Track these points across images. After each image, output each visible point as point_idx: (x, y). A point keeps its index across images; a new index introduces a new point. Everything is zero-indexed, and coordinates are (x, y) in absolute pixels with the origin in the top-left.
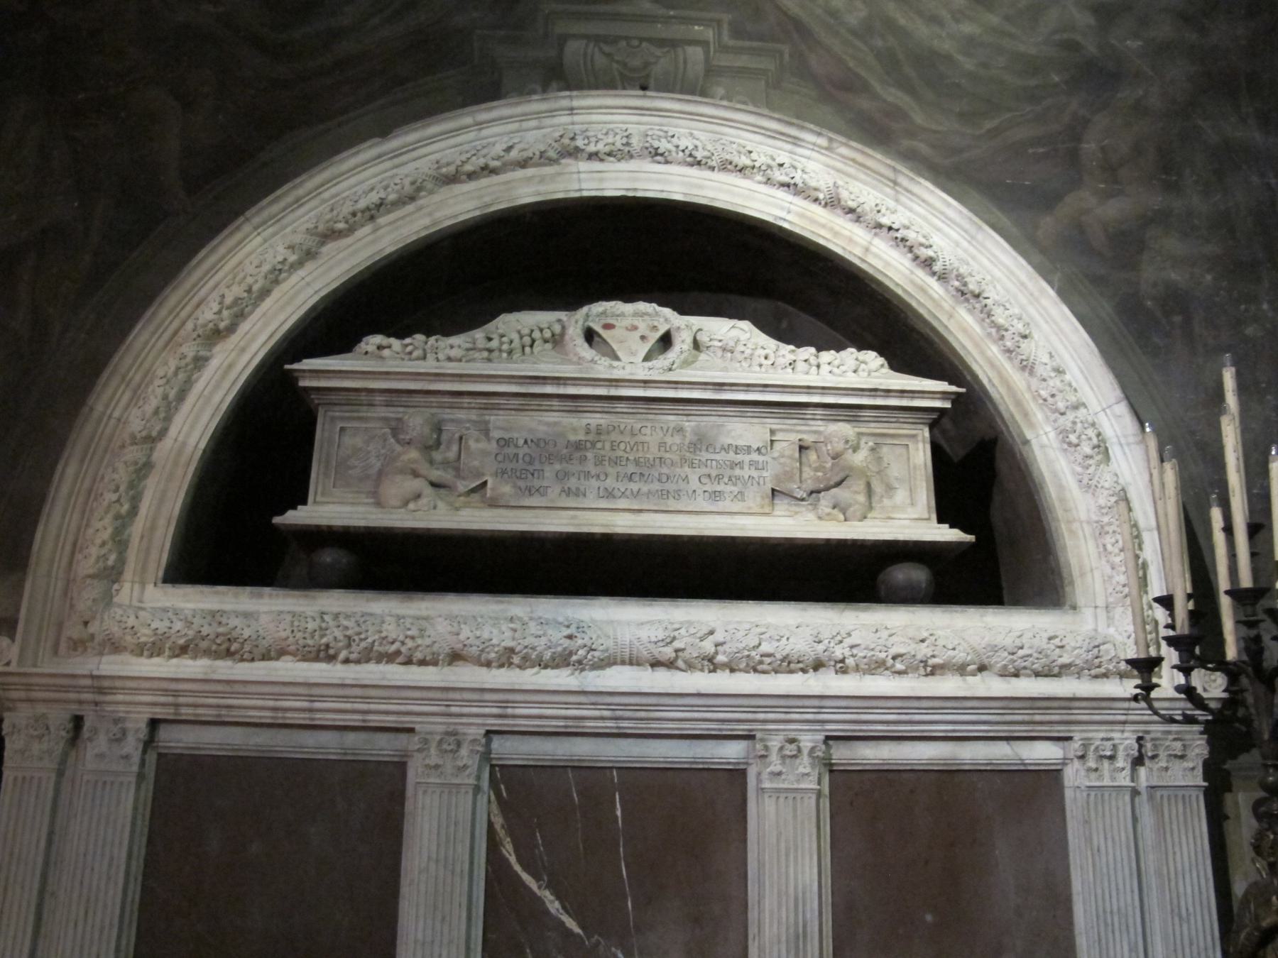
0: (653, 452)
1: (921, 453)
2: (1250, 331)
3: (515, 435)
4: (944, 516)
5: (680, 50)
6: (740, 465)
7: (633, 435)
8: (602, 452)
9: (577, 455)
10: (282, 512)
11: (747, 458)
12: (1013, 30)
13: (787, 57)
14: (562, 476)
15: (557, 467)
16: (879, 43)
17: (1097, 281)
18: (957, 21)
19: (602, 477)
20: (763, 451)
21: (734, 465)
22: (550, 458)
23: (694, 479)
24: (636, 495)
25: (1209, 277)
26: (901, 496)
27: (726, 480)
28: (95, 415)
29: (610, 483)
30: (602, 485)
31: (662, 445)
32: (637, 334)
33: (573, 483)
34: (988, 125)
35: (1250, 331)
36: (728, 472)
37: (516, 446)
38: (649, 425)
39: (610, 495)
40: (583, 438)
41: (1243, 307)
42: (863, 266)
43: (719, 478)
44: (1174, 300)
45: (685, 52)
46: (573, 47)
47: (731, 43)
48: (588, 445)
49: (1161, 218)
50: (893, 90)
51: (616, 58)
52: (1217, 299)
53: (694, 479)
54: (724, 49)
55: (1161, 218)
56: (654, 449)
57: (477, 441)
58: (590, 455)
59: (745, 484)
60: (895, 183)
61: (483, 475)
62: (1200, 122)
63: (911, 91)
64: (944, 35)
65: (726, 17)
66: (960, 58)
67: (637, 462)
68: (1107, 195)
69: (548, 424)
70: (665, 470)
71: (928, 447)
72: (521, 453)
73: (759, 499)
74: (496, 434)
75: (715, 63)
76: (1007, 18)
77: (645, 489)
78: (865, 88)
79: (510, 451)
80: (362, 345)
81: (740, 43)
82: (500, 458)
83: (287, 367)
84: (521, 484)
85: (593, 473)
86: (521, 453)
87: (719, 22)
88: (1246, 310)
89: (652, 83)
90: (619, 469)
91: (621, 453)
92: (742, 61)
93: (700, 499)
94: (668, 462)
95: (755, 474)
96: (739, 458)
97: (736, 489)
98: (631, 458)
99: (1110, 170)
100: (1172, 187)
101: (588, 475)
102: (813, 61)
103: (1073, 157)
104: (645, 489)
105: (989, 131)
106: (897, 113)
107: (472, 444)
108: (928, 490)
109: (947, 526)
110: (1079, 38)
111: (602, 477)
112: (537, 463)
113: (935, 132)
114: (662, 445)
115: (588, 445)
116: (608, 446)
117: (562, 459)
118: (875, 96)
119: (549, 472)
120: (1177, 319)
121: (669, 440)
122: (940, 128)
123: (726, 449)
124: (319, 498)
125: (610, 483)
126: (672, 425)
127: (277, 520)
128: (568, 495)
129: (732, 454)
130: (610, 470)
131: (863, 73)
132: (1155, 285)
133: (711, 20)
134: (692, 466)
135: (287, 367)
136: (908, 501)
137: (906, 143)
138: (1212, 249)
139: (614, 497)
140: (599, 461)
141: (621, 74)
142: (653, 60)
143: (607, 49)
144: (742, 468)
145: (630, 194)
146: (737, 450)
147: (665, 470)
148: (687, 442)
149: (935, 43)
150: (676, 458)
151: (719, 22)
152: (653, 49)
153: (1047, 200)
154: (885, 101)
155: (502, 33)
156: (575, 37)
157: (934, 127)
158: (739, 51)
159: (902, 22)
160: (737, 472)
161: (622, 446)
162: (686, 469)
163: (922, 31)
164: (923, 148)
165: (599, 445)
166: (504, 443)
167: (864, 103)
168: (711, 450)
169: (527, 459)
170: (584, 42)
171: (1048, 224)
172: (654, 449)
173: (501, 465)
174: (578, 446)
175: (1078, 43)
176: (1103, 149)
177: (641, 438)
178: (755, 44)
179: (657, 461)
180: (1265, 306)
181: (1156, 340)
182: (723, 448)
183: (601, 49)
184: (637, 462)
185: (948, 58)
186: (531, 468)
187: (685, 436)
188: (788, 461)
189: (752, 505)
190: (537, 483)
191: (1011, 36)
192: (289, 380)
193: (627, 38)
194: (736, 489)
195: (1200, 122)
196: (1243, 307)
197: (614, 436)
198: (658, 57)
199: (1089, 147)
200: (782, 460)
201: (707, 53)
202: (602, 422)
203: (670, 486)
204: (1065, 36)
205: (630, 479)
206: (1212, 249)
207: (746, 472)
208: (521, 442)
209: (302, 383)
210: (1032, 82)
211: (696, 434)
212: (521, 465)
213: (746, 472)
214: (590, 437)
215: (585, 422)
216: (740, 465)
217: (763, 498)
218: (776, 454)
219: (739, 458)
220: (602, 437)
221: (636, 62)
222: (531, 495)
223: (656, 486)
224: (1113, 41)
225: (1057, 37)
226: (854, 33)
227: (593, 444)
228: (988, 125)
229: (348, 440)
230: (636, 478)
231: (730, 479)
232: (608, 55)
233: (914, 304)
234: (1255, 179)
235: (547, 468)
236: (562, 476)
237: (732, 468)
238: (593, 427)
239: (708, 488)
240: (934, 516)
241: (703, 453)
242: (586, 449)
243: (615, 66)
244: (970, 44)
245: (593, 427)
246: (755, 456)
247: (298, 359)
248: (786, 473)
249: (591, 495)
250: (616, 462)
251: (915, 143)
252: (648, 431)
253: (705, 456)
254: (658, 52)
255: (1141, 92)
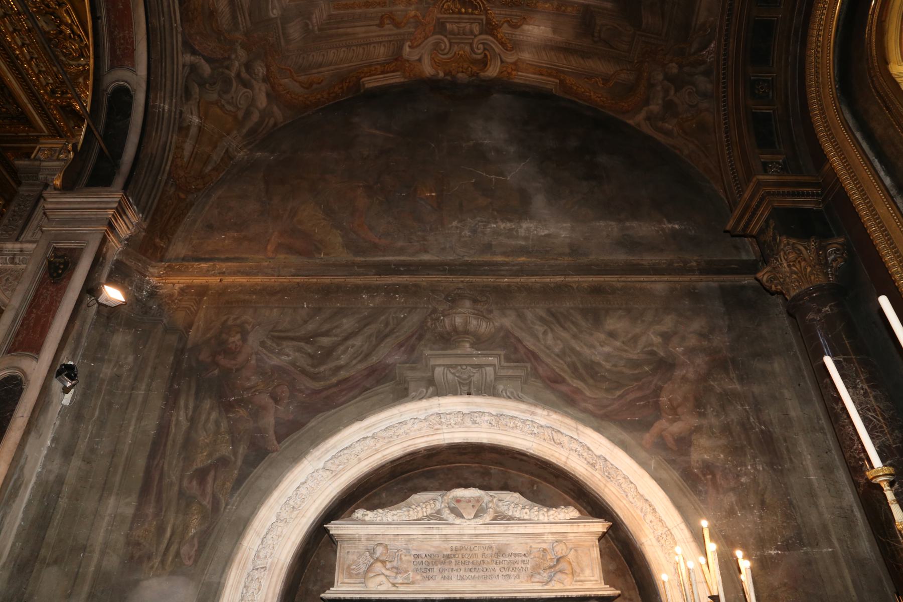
0: (480, 559)
1: (595, 552)
2: (743, 480)
3: (421, 553)
4: (608, 579)
5: (483, 369)
6: (517, 562)
7: (471, 551)
8: (458, 559)
9: (448, 561)
10: (324, 592)
11: (520, 559)
12: (626, 348)
13: (529, 369)
14: (441, 571)
15: (439, 566)
16: (569, 359)
17: (672, 462)
18: (602, 346)
19: (459, 570)
20: (527, 555)
21: (514, 562)
22: (436, 563)
23: (497, 569)
24: (473, 578)
25: (722, 456)
26: (588, 572)
27: (511, 569)
28: (244, 547)
29: (462, 573)
30: (458, 574)
31: (483, 554)
32: (471, 504)
33: (446, 574)
34: (618, 393)
35: (743, 480)
36: (512, 566)
37: (422, 558)
38: (478, 546)
39: (462, 578)
40: (449, 552)
41: (739, 469)
42: (565, 468)
43: (508, 568)
44: (708, 468)
45: (485, 370)
46: (439, 371)
47: (506, 364)
48: (452, 556)
49: (698, 430)
50: (575, 381)
51: (457, 375)
52: (727, 466)
53: (497, 569)
54: (503, 368)
55: (698, 430)
56: (480, 556)
57: (405, 556)
58: (453, 560)
59: (519, 571)
60: (577, 429)
61: (408, 571)
62: (712, 383)
63: (583, 380)
64: (596, 353)
65: (502, 353)
66: (604, 363)
67: (473, 563)
68: (674, 421)
69: (434, 547)
70: (485, 566)
71: (598, 549)
72: (424, 560)
73: (526, 578)
74: (413, 553)
75: (499, 374)
76: (623, 343)
77: (477, 575)
78: (563, 381)
79: (420, 560)
80: (356, 514)
81: (508, 364)
82: (415, 563)
83: (325, 526)
84: (424, 575)
85: (455, 569)
86: (424, 560)
87: (499, 355)
88: (741, 470)
89: (472, 391)
90: (466, 566)
91: (466, 559)
92: (510, 372)
93: (500, 578)
94: (486, 562)
95: (523, 566)
96: (516, 559)
97: (516, 574)
98: (471, 561)
99: (674, 409)
100: (702, 415)
101: (452, 570)
102: (541, 370)
103: (657, 406)
104: (477, 575)
105: (619, 396)
106: (577, 391)
107: (403, 557)
108: (599, 569)
109: (608, 586)
110: (655, 349)
111: (459, 570)
112: (431, 565)
113: (595, 399)
114: (483, 554)
115: (452, 556)
116: (460, 556)
117: (441, 563)
118: (569, 385)
119: (436, 569)
120: (709, 477)
121: (486, 552)
122: (597, 397)
123: (510, 555)
124: (339, 585)
125: (462, 573)
126: (487, 545)
127: (322, 595)
128: (444, 579)
129: (513, 557)
130: (463, 567)
131: (562, 374)
132: (698, 462)
133: (497, 355)
134: (496, 563)
135: (325, 526)
136: (591, 575)
137: (583, 405)
138: (723, 442)
139: (464, 579)
140: (457, 563)
141: (459, 381)
142: (472, 375)
143: (453, 371)
144: (518, 564)
145: (465, 441)
146: (515, 555)
147: (485, 566)
148: (494, 553)
149: (593, 357)
150: (489, 560)
151: (499, 355)
152: (472, 369)
153: (645, 426)
154: (572, 386)
155: (408, 365)
156: (439, 366)
157: (594, 396)
158: (508, 368)
159: (578, 349)
160: (516, 565)
161: (466, 556)
162: (494, 565)
163: (586, 351)
164: (590, 407)
165: (457, 556)
166: (417, 556)
167: (563, 388)
168: (504, 556)
169: (427, 563)
170: (443, 368)
171: (648, 437)
172: (480, 556)
173: (416, 567)
174: (448, 557)
175: (655, 351)
176: (669, 400)
177: (474, 552)
178: (515, 364)
179: (482, 562)
180: (749, 467)
181: (701, 488)
182: (509, 555)
183: (450, 371)
184: (473, 563)
185: (599, 364)
186: (428, 568)
187: (493, 550)
188: (537, 559)
189: (523, 580)
190: (431, 574)
191: (626, 351)
192: (327, 531)
193: (461, 365)
194: (516, 574)
195: (712, 383)
196: (739, 469)
197: (463, 552)
198: (475, 373)
199: (664, 399)
200: (535, 559)
201: (495, 370)
202: (457, 545)
203: (488, 574)
204: (650, 349)
205: (471, 571)
206: (723, 442)
207: (520, 565)
208: (424, 556)
209: (331, 533)
210: (636, 372)
211: (497, 549)
212: (424, 566)
213: (520, 565)
214: (453, 552)
215: (450, 546)
216: (517, 562)
217: (527, 577)
218: (532, 557)
219: (516, 559)
220: (458, 552)
221: (465, 376)
222: (429, 580)
223: (482, 574)
224: (671, 349)
225: (646, 349)
226: (558, 356)
227: (454, 555)
228: (618, 393)
229: (351, 557)
230: (473, 570)
231: (513, 569)
232: (453, 374)
233: (588, 484)
234: (739, 407)
235: (435, 567)
236: (441, 571)
237: (514, 564)
238: (454, 548)
239: (504, 573)
240: (603, 582)
241: (501, 558)
242: (451, 558)
243: (456, 378)
244: (608, 357)
245: (454, 548)
246: (523, 558)
247: (329, 522)
248: (537, 564)
249: (454, 579)
250: (464, 563)
251: (587, 405)
252: (477, 549)
253: (501, 559)
254: (474, 371)
255: (685, 372)
